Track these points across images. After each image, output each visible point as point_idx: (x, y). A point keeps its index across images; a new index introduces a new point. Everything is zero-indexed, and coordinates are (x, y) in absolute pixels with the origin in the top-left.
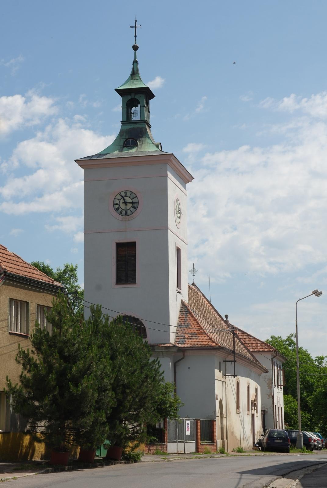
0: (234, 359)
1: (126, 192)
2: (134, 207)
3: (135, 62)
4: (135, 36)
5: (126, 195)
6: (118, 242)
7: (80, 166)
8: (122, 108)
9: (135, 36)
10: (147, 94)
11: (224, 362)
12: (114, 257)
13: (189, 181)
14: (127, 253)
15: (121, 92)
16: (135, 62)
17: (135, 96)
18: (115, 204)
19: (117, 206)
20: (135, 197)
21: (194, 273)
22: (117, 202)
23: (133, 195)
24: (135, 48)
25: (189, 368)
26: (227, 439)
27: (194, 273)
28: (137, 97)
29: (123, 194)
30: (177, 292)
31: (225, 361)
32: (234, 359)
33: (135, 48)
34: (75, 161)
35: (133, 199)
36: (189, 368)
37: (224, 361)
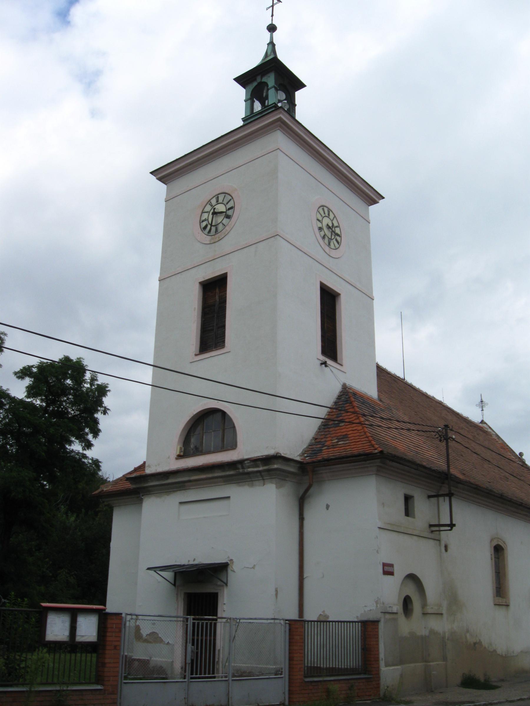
0: (450, 491)
1: (218, 197)
2: (228, 217)
3: (272, 44)
4: (272, 16)
5: (217, 201)
6: (200, 281)
7: (160, 179)
8: (245, 101)
9: (272, 16)
10: (291, 84)
11: (434, 500)
12: (195, 308)
13: (375, 202)
14: (217, 297)
15: (243, 80)
16: (272, 44)
17: (262, 78)
18: (203, 221)
19: (204, 224)
20: (230, 200)
21: (482, 407)
22: (205, 216)
23: (226, 196)
24: (272, 28)
25: (328, 507)
26: (445, 659)
27: (482, 407)
28: (264, 80)
29: (214, 202)
30: (322, 364)
31: (437, 496)
32: (450, 491)
33: (272, 28)
34: (151, 173)
35: (227, 203)
36: (328, 507)
37: (429, 497)
